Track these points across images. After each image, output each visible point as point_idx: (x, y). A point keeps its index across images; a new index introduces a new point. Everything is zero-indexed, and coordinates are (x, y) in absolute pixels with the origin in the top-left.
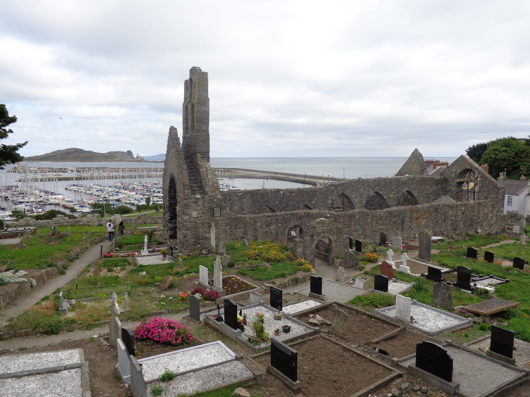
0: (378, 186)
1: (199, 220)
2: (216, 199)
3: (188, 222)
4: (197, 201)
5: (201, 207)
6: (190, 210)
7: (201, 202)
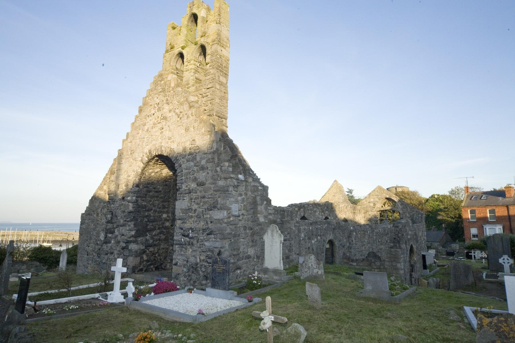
0: (328, 211)
1: (240, 220)
2: (261, 186)
3: (226, 223)
4: (239, 184)
5: (243, 197)
6: (230, 199)
7: (244, 188)
